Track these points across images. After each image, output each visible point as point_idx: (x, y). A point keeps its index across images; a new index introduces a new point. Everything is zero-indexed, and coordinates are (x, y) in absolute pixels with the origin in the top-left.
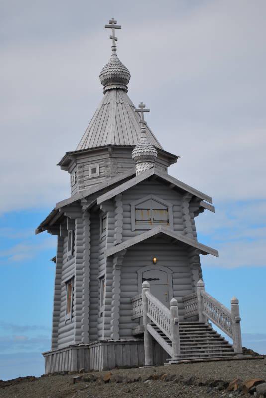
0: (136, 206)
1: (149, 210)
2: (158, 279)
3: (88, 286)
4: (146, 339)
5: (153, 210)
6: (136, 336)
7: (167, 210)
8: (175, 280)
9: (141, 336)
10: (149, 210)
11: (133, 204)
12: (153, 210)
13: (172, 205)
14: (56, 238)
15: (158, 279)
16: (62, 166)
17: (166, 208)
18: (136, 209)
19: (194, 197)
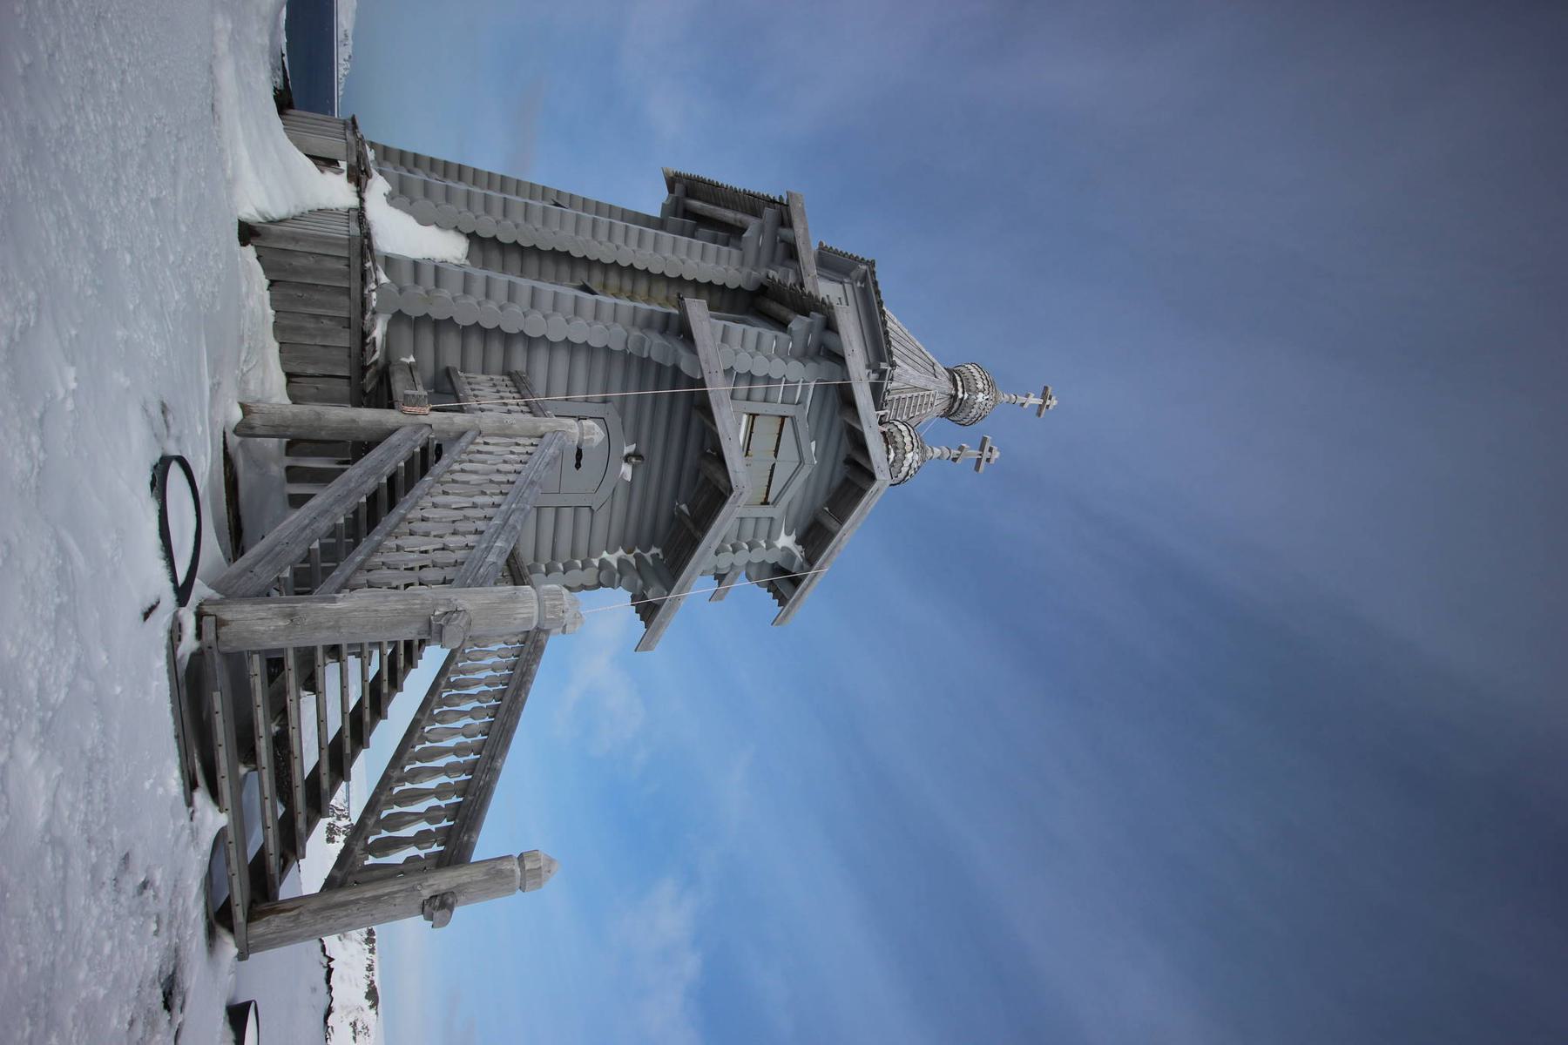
0: (793, 418)
1: (776, 456)
2: (578, 466)
3: (558, 248)
4: (368, 416)
5: (774, 465)
6: (384, 375)
7: (765, 503)
8: (567, 515)
9: (382, 397)
10: (776, 456)
11: (802, 414)
12: (774, 465)
13: (776, 518)
14: (656, 213)
15: (578, 466)
16: (820, 253)
17: (770, 499)
18: (783, 418)
19: (796, 582)
